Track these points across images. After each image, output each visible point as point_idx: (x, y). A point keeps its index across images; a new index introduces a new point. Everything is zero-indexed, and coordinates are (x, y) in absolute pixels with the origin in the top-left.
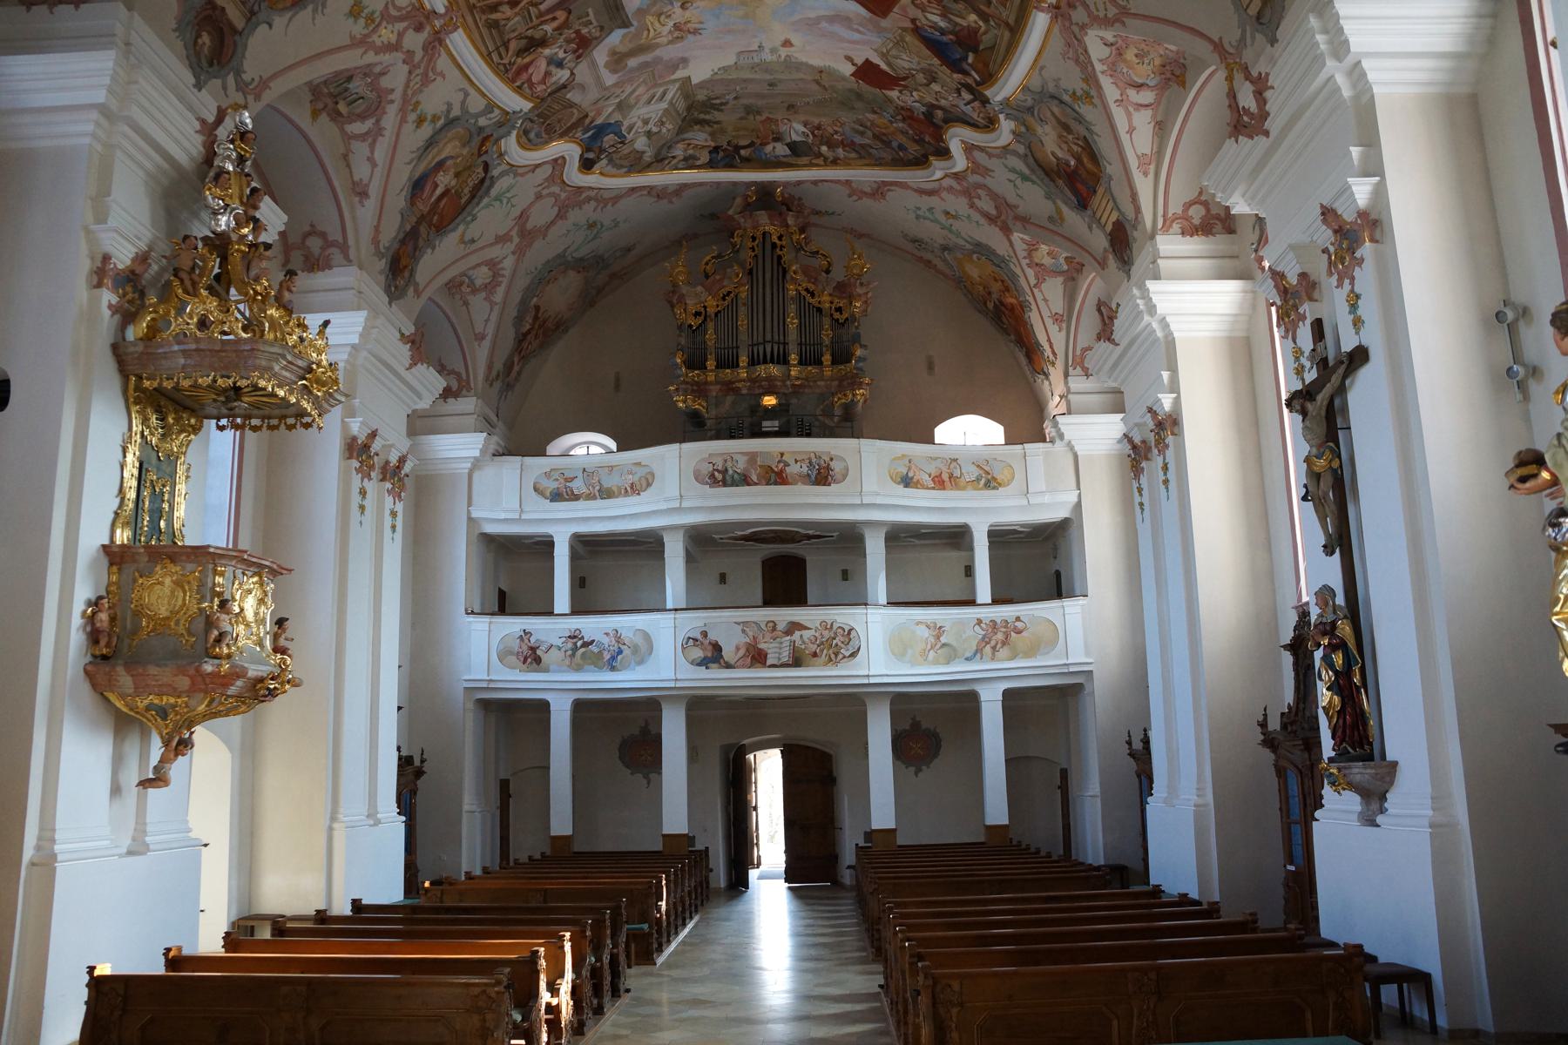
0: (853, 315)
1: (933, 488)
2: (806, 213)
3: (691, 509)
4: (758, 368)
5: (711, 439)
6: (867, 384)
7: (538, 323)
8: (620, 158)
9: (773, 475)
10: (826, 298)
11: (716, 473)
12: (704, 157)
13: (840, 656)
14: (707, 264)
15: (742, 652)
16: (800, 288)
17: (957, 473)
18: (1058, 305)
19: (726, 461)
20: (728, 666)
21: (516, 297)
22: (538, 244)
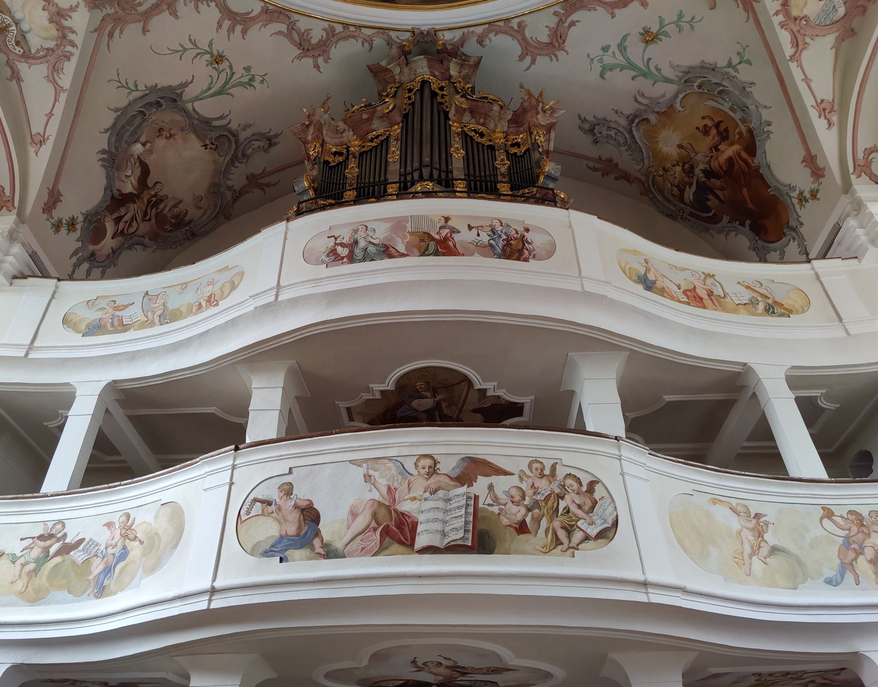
1: (688, 304)
3: (294, 302)
11: (339, 249)
13: (578, 536)
15: (363, 520)
16: (465, 129)
17: (718, 291)
18: (825, 89)
20: (330, 553)
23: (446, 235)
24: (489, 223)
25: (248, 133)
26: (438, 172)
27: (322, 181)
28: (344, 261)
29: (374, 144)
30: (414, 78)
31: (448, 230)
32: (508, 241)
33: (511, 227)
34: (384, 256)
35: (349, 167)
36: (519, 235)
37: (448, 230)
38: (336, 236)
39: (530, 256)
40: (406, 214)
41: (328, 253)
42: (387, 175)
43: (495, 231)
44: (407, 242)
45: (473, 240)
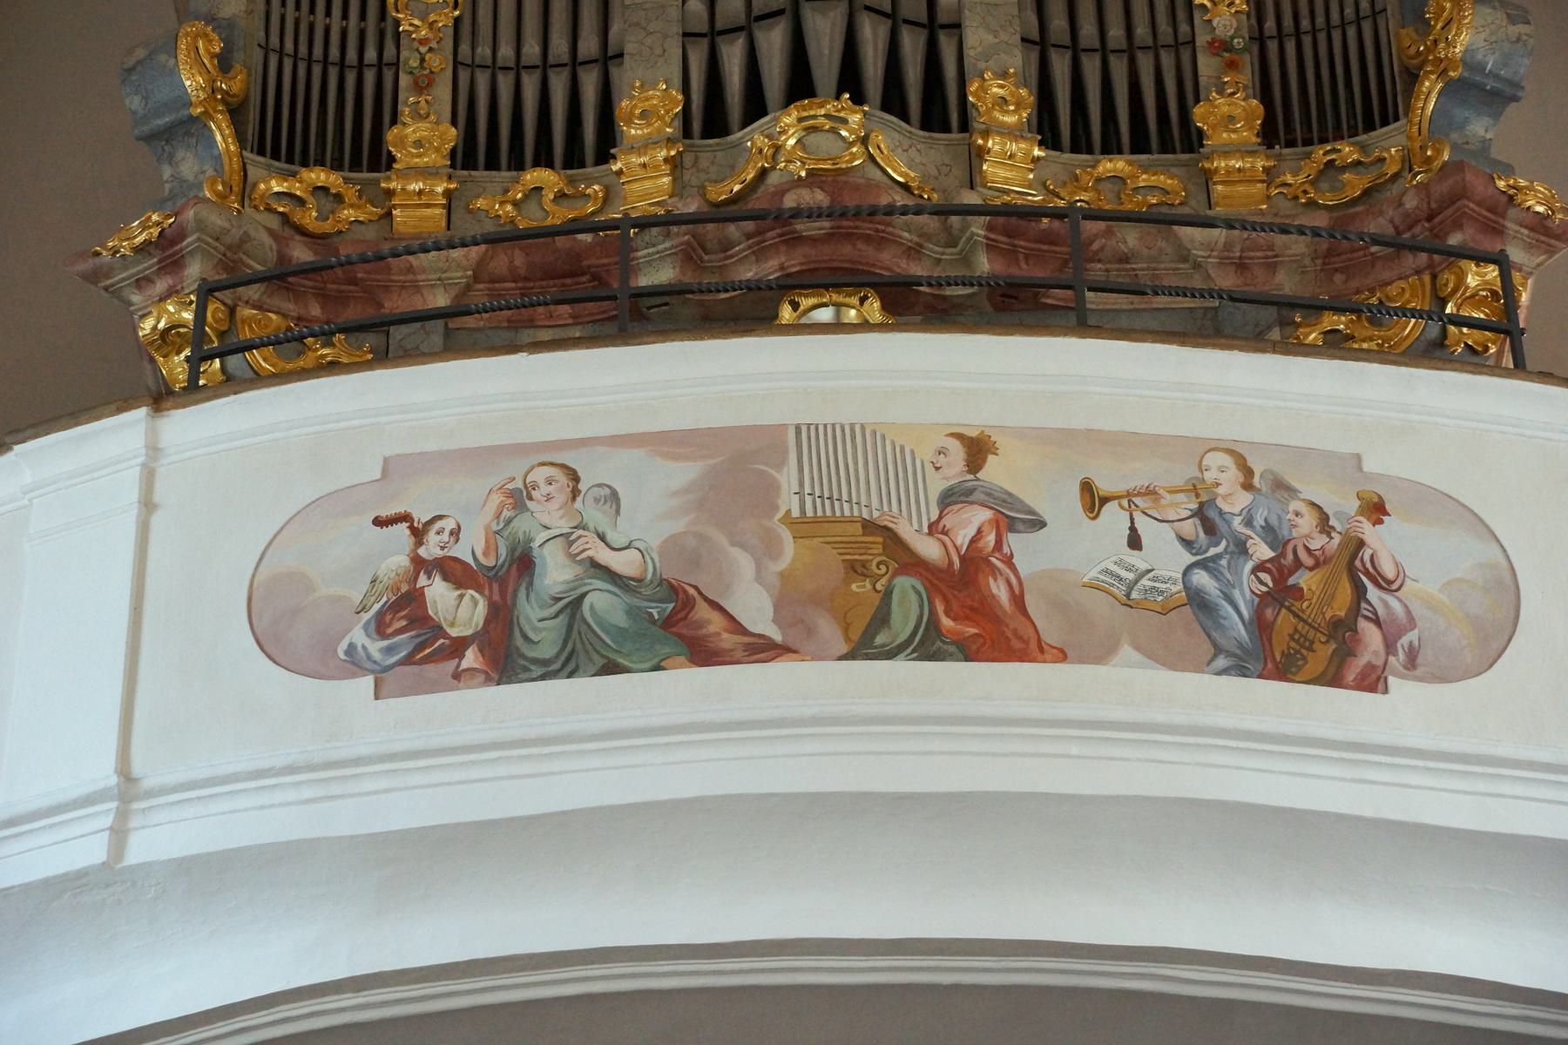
4: (755, 138)
9: (907, 589)
11: (438, 593)
19: (519, 499)
23: (973, 541)
24: (1182, 473)
26: (884, 28)
27: (266, 49)
28: (465, 664)
31: (984, 515)
32: (1280, 570)
33: (1292, 491)
34: (667, 650)
36: (1337, 539)
37: (984, 515)
38: (420, 516)
39: (1392, 659)
40: (769, 418)
41: (380, 616)
42: (615, 28)
43: (1218, 520)
44: (782, 575)
45: (1106, 571)
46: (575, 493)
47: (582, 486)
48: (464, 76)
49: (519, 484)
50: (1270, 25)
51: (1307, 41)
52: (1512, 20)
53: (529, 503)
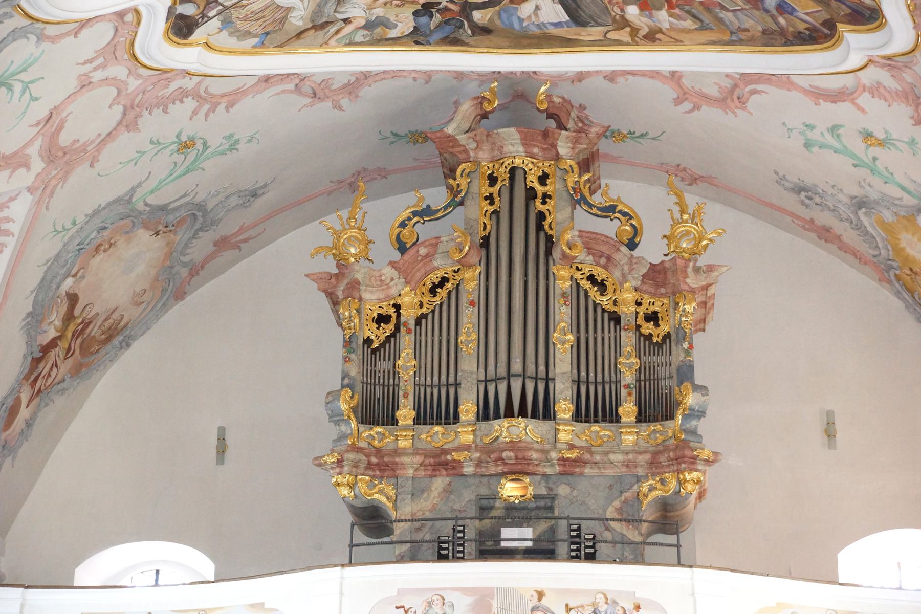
0: (679, 329)
2: (594, 130)
4: (496, 424)
5: (401, 559)
6: (707, 462)
7: (72, 328)
8: (246, 19)
10: (629, 296)
12: (405, 22)
14: (403, 225)
16: (578, 275)
19: (430, 604)
21: (32, 277)
22: (81, 173)
25: (221, 197)
27: (363, 383)
29: (437, 299)
30: (499, 158)
35: (403, 355)
38: (407, 607)
46: (444, 603)
47: (445, 602)
48: (417, 389)
49: (430, 600)
50: (642, 377)
51: (652, 382)
52: (703, 395)
53: (433, 606)
